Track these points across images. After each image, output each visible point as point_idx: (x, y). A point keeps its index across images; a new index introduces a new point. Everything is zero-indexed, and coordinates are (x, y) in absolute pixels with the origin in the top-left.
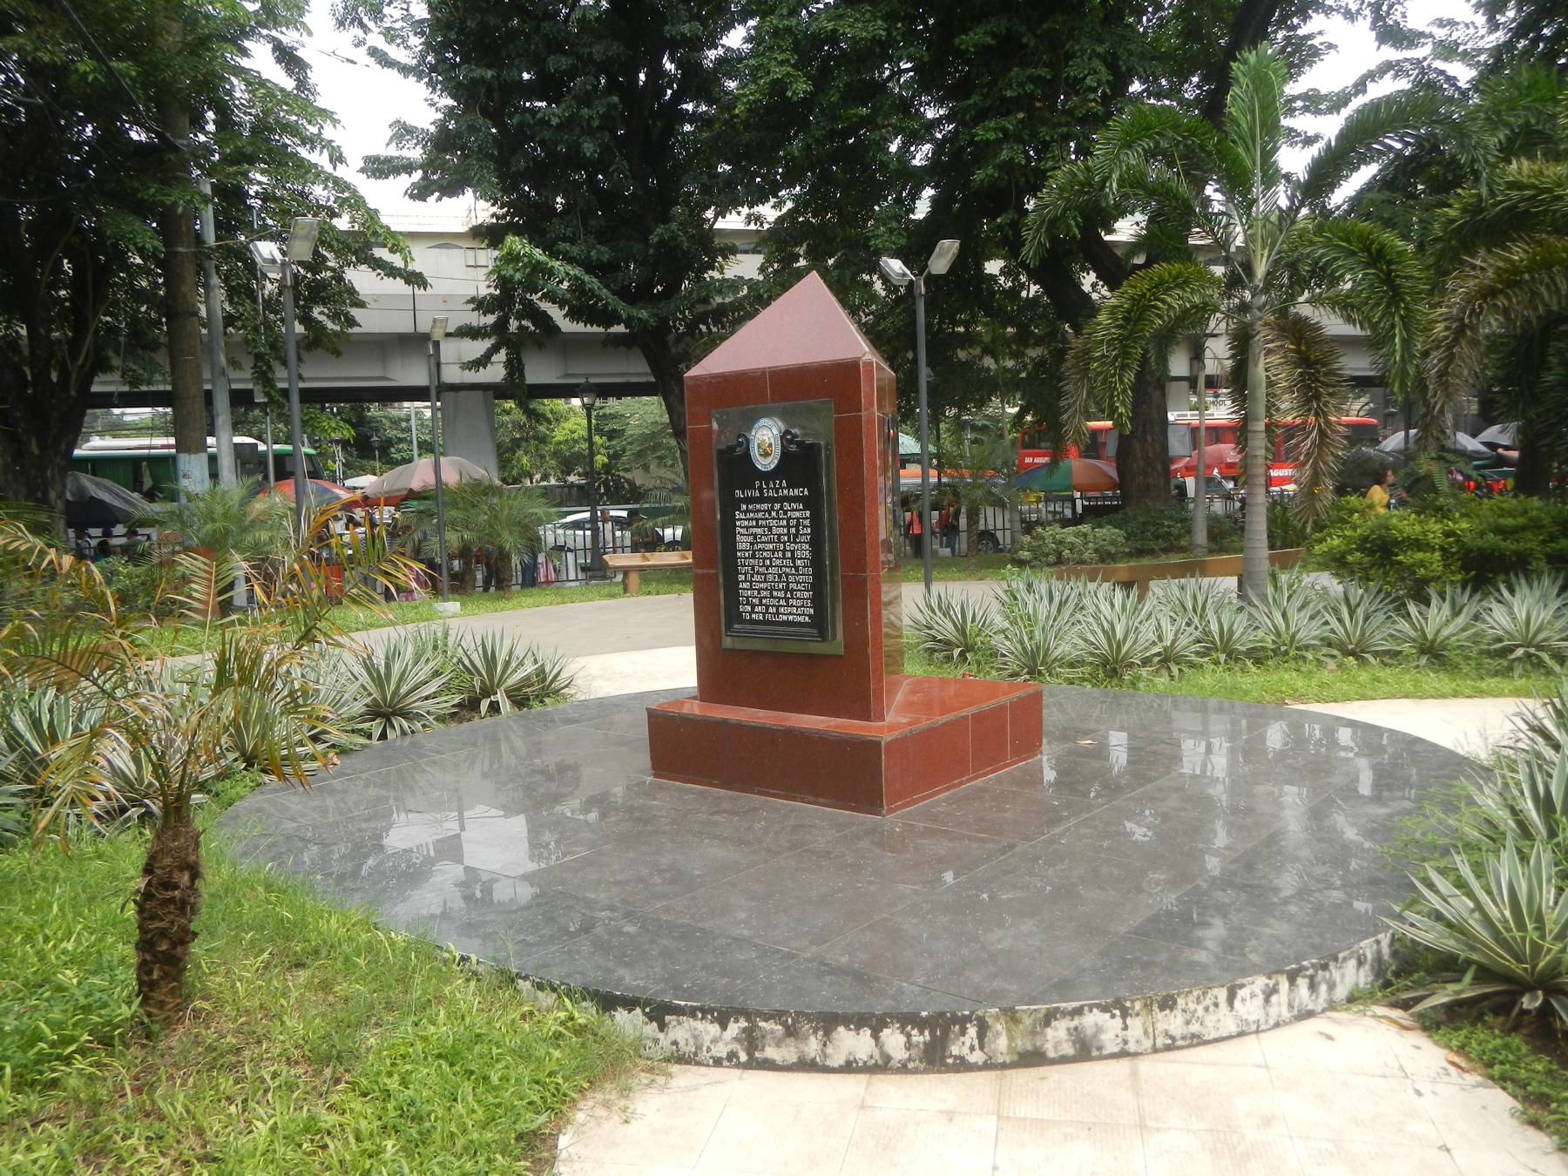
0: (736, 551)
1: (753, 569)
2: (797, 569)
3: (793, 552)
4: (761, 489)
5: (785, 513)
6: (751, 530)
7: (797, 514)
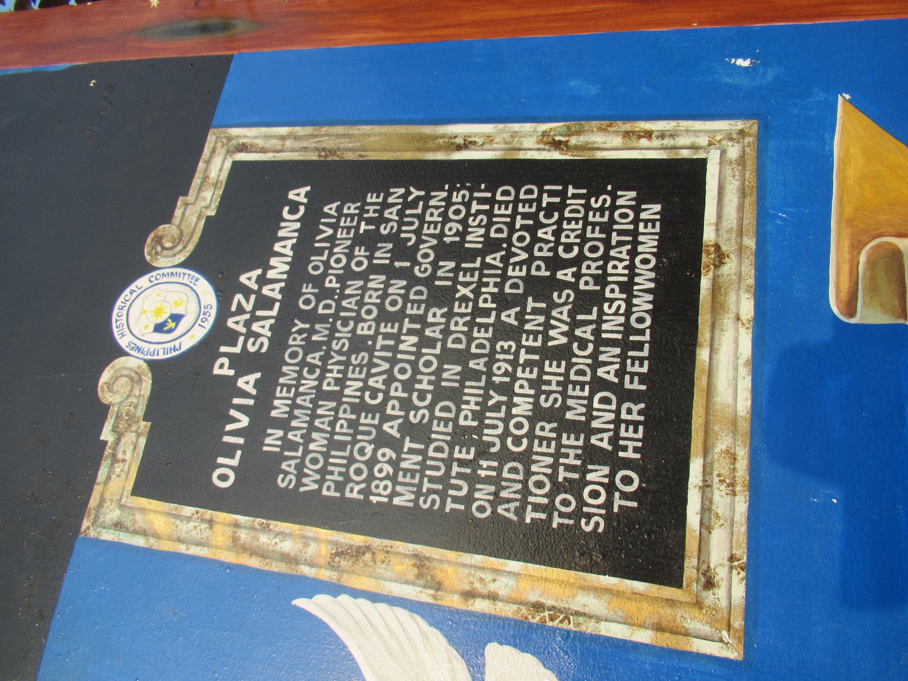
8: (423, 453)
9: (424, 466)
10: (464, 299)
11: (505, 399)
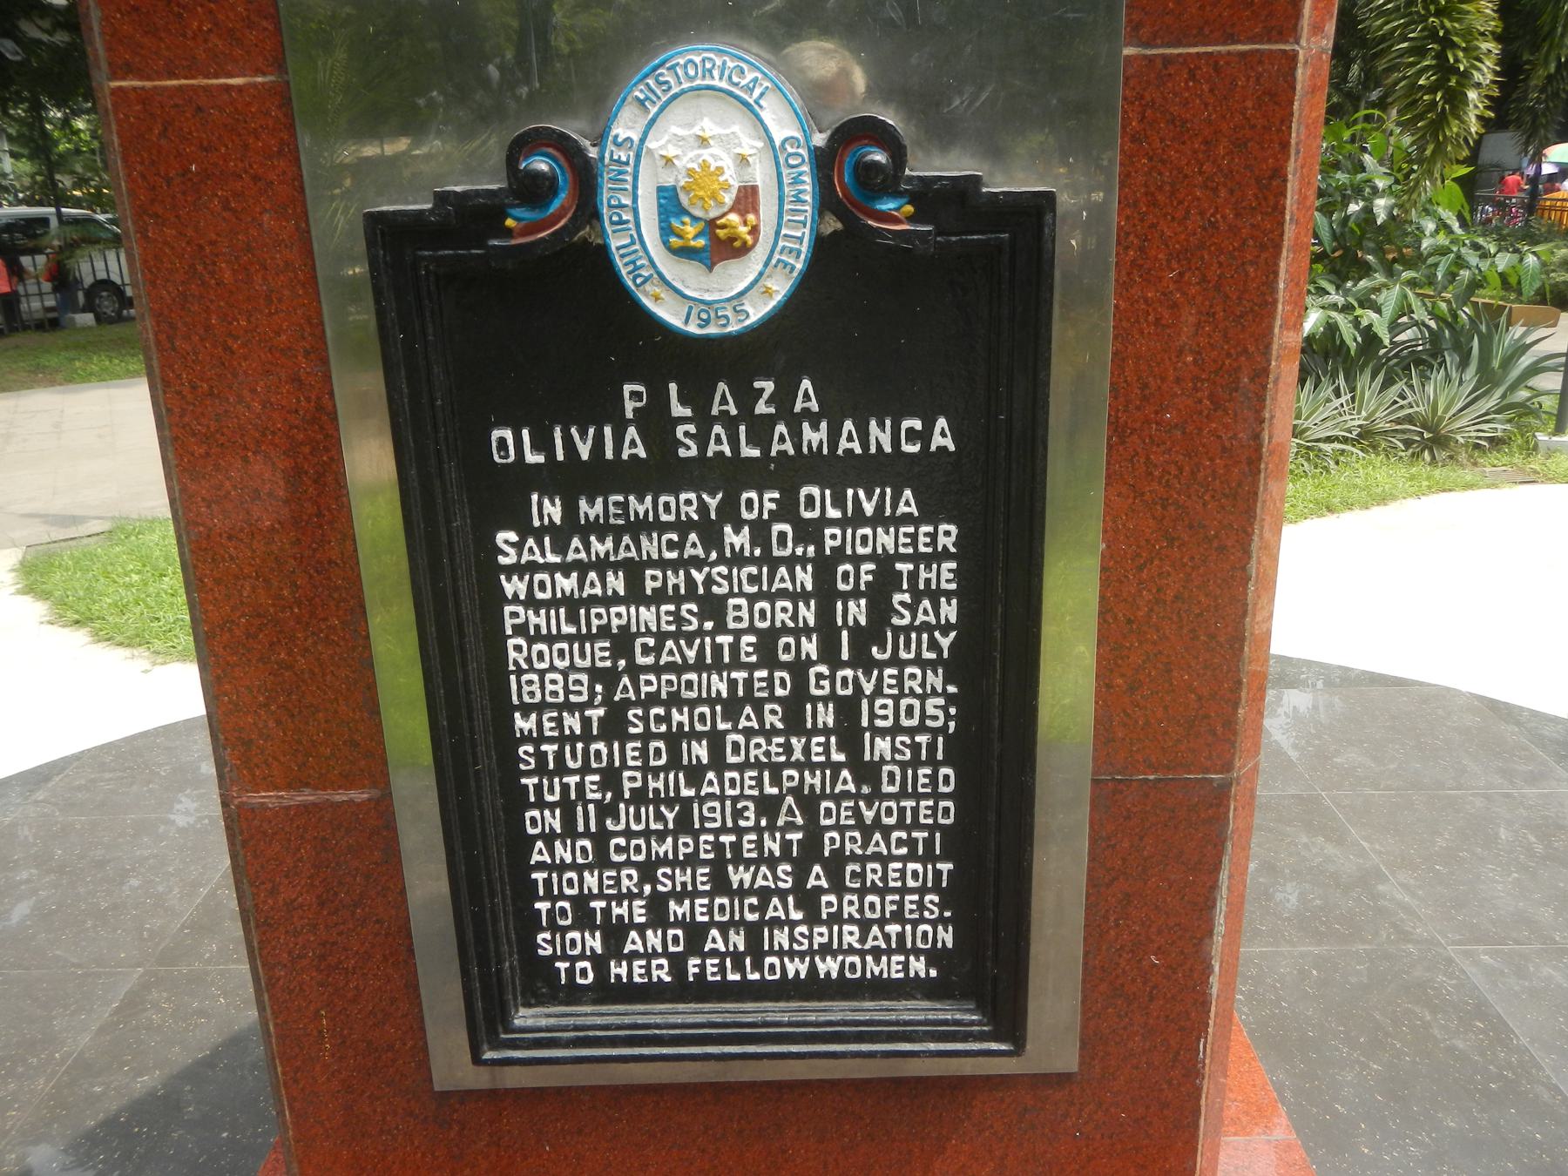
0: (503, 710)
1: (611, 778)
2: (867, 772)
3: (847, 708)
4: (656, 423)
5: (809, 532)
6: (597, 617)
7: (886, 540)
8: (587, 737)
9: (573, 739)
11: (671, 826)
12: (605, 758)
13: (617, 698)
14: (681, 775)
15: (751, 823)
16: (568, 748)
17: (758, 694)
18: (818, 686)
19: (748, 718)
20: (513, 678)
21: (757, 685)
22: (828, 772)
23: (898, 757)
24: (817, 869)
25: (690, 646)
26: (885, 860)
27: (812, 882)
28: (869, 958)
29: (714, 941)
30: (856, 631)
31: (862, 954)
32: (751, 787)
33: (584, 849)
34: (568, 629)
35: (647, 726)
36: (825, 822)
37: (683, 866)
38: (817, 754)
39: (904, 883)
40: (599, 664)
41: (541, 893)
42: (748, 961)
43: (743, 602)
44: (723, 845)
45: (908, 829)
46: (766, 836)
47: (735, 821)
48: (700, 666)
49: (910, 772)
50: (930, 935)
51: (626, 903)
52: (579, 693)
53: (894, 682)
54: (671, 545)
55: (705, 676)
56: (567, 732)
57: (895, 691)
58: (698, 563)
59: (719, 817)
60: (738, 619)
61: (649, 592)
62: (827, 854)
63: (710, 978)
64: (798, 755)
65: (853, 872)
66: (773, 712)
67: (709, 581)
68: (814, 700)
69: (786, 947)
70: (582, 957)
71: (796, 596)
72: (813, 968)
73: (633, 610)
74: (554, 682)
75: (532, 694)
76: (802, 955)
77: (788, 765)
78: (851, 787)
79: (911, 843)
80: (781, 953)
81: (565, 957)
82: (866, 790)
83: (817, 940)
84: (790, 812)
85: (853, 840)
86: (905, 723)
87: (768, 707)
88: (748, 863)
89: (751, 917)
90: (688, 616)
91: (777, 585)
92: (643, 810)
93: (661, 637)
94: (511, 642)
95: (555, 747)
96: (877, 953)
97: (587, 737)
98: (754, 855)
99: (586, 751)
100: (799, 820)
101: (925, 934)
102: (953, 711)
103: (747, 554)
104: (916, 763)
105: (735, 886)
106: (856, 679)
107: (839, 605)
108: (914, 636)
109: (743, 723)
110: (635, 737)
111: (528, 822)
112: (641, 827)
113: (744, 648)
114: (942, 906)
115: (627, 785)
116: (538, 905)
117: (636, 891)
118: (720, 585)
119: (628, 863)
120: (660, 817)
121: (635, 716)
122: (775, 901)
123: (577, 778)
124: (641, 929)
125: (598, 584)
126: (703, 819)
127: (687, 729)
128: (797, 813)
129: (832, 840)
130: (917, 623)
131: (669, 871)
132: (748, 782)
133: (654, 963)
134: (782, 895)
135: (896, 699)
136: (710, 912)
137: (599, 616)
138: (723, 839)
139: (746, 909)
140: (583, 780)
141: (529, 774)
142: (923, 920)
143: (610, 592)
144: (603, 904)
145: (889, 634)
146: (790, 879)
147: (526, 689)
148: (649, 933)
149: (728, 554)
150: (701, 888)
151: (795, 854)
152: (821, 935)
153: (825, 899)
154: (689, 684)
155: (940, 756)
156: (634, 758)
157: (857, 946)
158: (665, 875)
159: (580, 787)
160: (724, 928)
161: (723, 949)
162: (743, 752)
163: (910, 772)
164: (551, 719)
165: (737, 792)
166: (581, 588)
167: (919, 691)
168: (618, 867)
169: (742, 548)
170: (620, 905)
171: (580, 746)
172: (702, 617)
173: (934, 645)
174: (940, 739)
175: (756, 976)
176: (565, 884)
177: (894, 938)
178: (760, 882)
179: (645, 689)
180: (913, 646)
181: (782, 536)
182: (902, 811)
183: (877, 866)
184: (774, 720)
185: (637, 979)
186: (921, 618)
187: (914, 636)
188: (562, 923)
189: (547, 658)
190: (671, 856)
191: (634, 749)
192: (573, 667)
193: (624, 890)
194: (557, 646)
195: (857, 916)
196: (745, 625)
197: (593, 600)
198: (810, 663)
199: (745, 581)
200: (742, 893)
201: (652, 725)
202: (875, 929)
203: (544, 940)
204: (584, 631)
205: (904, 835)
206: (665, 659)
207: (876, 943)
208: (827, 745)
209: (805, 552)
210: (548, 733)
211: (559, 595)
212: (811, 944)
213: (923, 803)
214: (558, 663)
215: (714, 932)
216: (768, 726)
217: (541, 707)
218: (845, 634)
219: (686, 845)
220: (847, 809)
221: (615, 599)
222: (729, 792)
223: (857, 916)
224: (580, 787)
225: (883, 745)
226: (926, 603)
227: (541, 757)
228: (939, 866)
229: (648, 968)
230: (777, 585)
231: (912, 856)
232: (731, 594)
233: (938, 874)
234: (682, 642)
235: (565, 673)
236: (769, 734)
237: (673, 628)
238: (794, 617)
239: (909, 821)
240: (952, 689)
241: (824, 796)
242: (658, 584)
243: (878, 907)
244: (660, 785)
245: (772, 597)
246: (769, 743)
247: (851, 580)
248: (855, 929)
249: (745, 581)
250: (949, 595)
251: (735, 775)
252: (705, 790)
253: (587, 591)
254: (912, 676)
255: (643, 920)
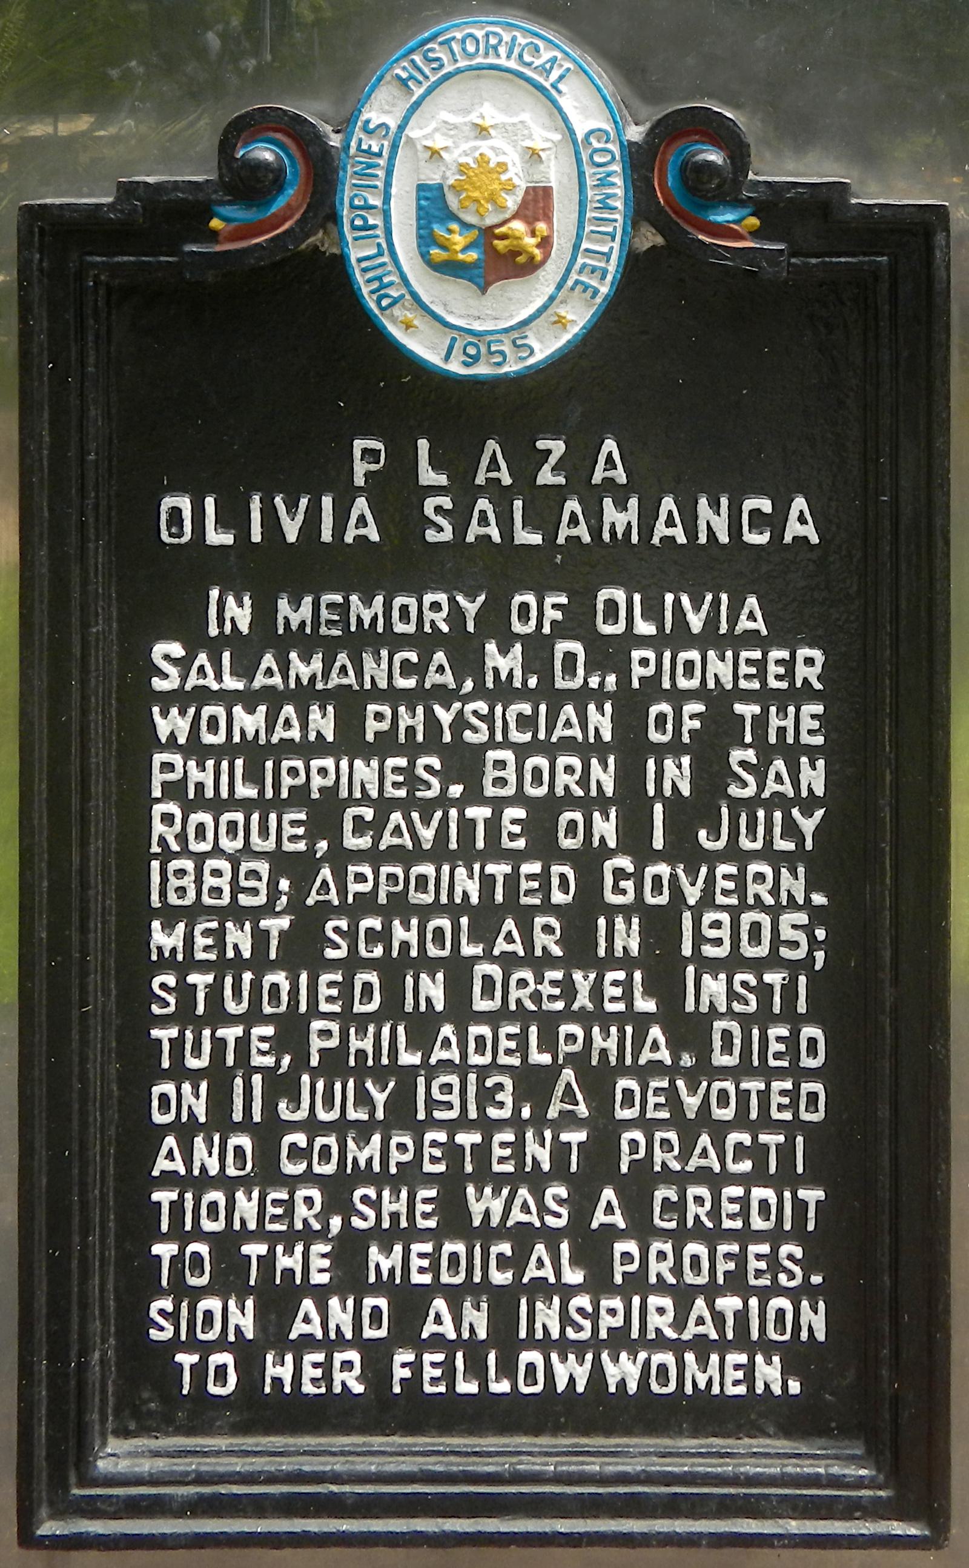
8: (260, 963)
9: (238, 964)
10: (569, 990)
12: (285, 998)
13: (310, 902)
14: (401, 1029)
15: (506, 1113)
16: (229, 980)
17: (525, 900)
18: (617, 890)
19: (509, 938)
20: (155, 865)
21: (524, 885)
22: (629, 1029)
23: (737, 1007)
24: (608, 1194)
25: (426, 821)
26: (716, 1181)
27: (599, 1218)
28: (690, 1357)
29: (438, 1320)
30: (675, 804)
31: (678, 1348)
32: (509, 1052)
33: (239, 1151)
34: (246, 791)
35: (353, 948)
36: (624, 1114)
37: (395, 1183)
38: (613, 999)
39: (747, 1222)
40: (288, 847)
41: (164, 1227)
42: (492, 1358)
43: (508, 755)
44: (462, 1147)
45: (754, 1129)
46: (529, 1135)
47: (481, 1109)
48: (439, 853)
49: (756, 1032)
50: (789, 1317)
51: (299, 1248)
52: (255, 892)
53: (730, 885)
54: (407, 668)
55: (446, 868)
56: (230, 954)
57: (733, 901)
58: (445, 695)
59: (457, 1103)
60: (501, 782)
61: (370, 737)
62: (624, 1169)
63: (428, 1389)
64: (583, 1000)
65: (666, 1200)
66: (548, 929)
67: (460, 723)
68: (611, 911)
69: (555, 1334)
70: (221, 1344)
71: (585, 749)
72: (597, 1373)
73: (344, 764)
74: (217, 873)
75: (181, 891)
76: (580, 1349)
77: (568, 1015)
78: (664, 1055)
79: (758, 1153)
80: (545, 1345)
81: (193, 1344)
82: (687, 1060)
83: (607, 1322)
84: (569, 1095)
85: (666, 1144)
86: (750, 951)
87: (539, 921)
88: (499, 1181)
89: (500, 1278)
90: (426, 776)
91: (559, 732)
92: (338, 1086)
93: (384, 806)
94: (158, 809)
95: (210, 978)
96: (702, 1347)
97: (260, 963)
98: (509, 1168)
99: (257, 985)
100: (582, 1110)
101: (781, 1313)
102: (821, 934)
103: (517, 684)
104: (764, 1017)
105: (477, 1223)
106: (674, 877)
107: (651, 764)
108: (761, 814)
109: (501, 946)
110: (333, 965)
111: (155, 1103)
112: (334, 1115)
113: (508, 827)
114: (808, 1265)
115: (316, 1044)
116: (157, 1249)
117: (317, 1226)
118: (475, 730)
119: (309, 1177)
120: (364, 1099)
121: (337, 930)
122: (540, 1249)
123: (239, 1031)
124: (321, 1295)
125: (295, 723)
126: (431, 1104)
127: (414, 953)
128: (580, 1097)
129: (633, 1143)
130: (766, 794)
131: (372, 1193)
132: (505, 1044)
133: (339, 1357)
134: (551, 1238)
135: (736, 913)
136: (435, 1268)
137: (293, 772)
138: (462, 1138)
139: (493, 1263)
140: (247, 1033)
141: (164, 1021)
142: (777, 1290)
143: (312, 737)
144: (262, 1249)
145: (725, 811)
146: (564, 1212)
147: (174, 882)
148: (334, 1303)
149: (490, 685)
150: (422, 1224)
151: (574, 1168)
152: (612, 1312)
153: (620, 1247)
154: (422, 880)
155: (802, 1008)
156: (330, 999)
157: (670, 1334)
158: (365, 1199)
159: (243, 1043)
160: (455, 1296)
161: (452, 1335)
162: (498, 994)
163: (756, 1032)
164: (207, 933)
165: (487, 1059)
166: (270, 728)
167: (769, 900)
168: (292, 1183)
169: (510, 675)
170: (289, 1251)
171: (247, 976)
172: (446, 777)
173: (791, 829)
174: (802, 979)
175: (502, 1387)
176: (204, 1211)
177: (730, 1322)
178: (517, 1216)
179: (354, 888)
180: (761, 830)
181: (570, 658)
182: (743, 1096)
183: (704, 1192)
184: (547, 942)
185: (308, 1388)
186: (772, 787)
187: (761, 814)
188: (193, 1281)
189: (210, 835)
190: (377, 1168)
191: (331, 984)
192: (247, 850)
193: (299, 1225)
194: (226, 817)
195: (671, 1280)
196: (510, 791)
197: (287, 747)
198: (606, 853)
199: (512, 725)
200: (488, 1233)
201: (362, 946)
202: (700, 1303)
203: (162, 1312)
204: (269, 794)
205: (746, 1139)
206: (387, 840)
207: (701, 1329)
208: (627, 985)
209: (602, 684)
210: (200, 956)
211: (237, 739)
212: (595, 1329)
213: (776, 1085)
214: (226, 844)
215: (440, 1304)
216: (538, 952)
217: (193, 913)
218: (658, 808)
219: (402, 1147)
220: (657, 1091)
221: (320, 747)
222: (475, 1059)
223: (671, 1280)
224: (243, 1043)
225: (714, 987)
226: (779, 765)
227: (185, 992)
228: (802, 1194)
229: (327, 1366)
230: (559, 732)
231: (758, 1177)
232: (491, 744)
233: (800, 1206)
234: (415, 816)
235: (235, 861)
236: (540, 963)
237: (402, 793)
238: (584, 781)
239: (754, 1115)
240: (819, 899)
241: (622, 1070)
242: (385, 726)
243: (705, 1265)
244: (368, 1045)
245: (552, 750)
246: (540, 980)
247: (669, 727)
248: (667, 1302)
249: (512, 725)
250: (812, 752)
251: (485, 1030)
252: (439, 1054)
253: (279, 734)
254: (760, 877)
255: (324, 1278)
